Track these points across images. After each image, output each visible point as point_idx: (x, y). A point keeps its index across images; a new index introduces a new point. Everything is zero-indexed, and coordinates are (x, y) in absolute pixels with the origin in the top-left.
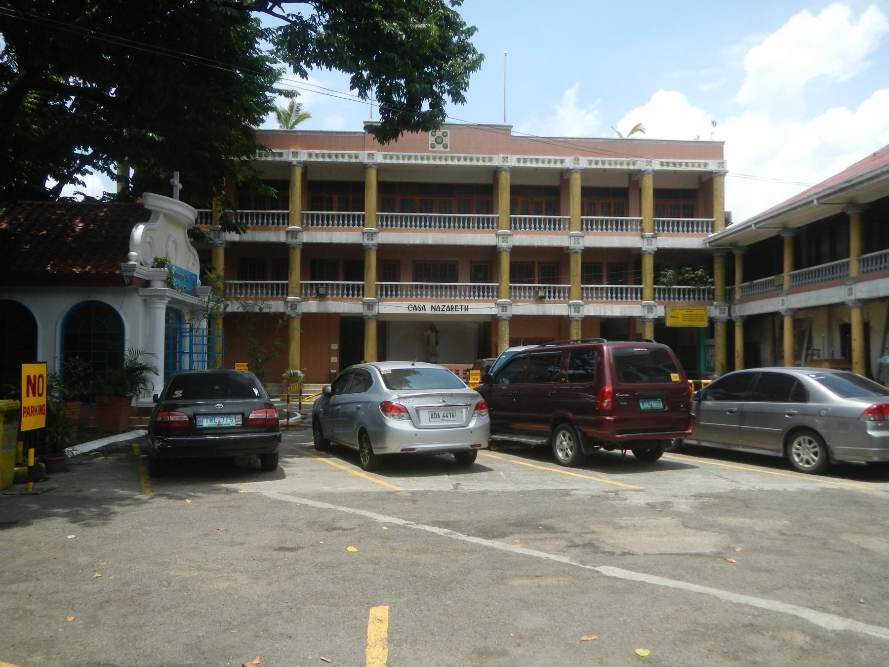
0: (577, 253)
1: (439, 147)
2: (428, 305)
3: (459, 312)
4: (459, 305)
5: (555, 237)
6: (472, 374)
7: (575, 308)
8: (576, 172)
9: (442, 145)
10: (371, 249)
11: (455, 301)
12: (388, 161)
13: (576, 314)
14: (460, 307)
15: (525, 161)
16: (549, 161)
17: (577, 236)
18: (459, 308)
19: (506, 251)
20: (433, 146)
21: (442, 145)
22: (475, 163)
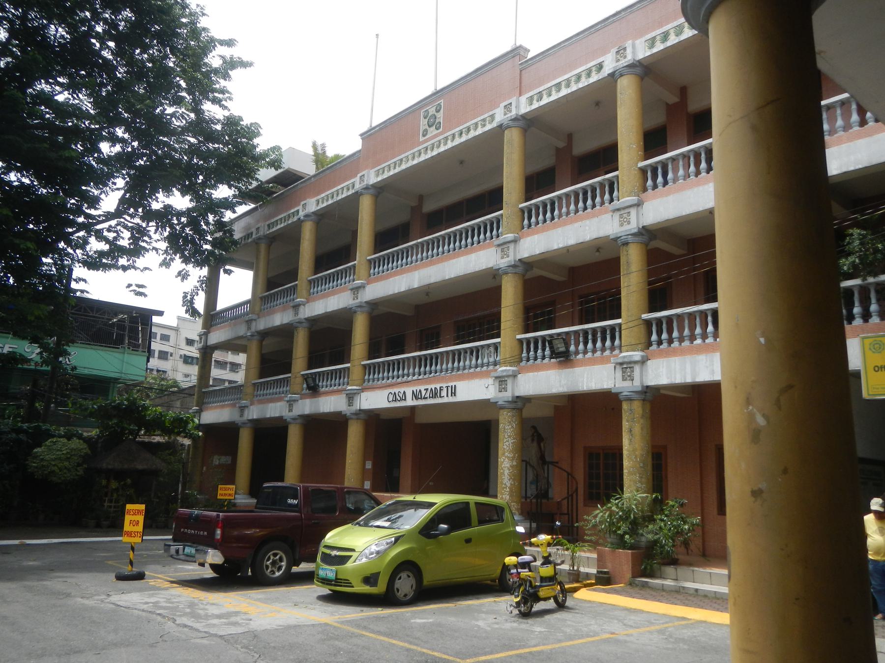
0: (626, 244)
1: (432, 131)
2: (409, 391)
3: (445, 400)
4: (444, 385)
5: (588, 222)
6: (129, 511)
7: (624, 371)
8: (621, 75)
9: (434, 127)
10: (355, 312)
11: (438, 382)
12: (386, 175)
13: (627, 384)
14: (445, 389)
15: (540, 96)
16: (578, 77)
17: (624, 208)
18: (444, 393)
19: (506, 273)
20: (425, 133)
21: (434, 127)
22: (472, 134)
